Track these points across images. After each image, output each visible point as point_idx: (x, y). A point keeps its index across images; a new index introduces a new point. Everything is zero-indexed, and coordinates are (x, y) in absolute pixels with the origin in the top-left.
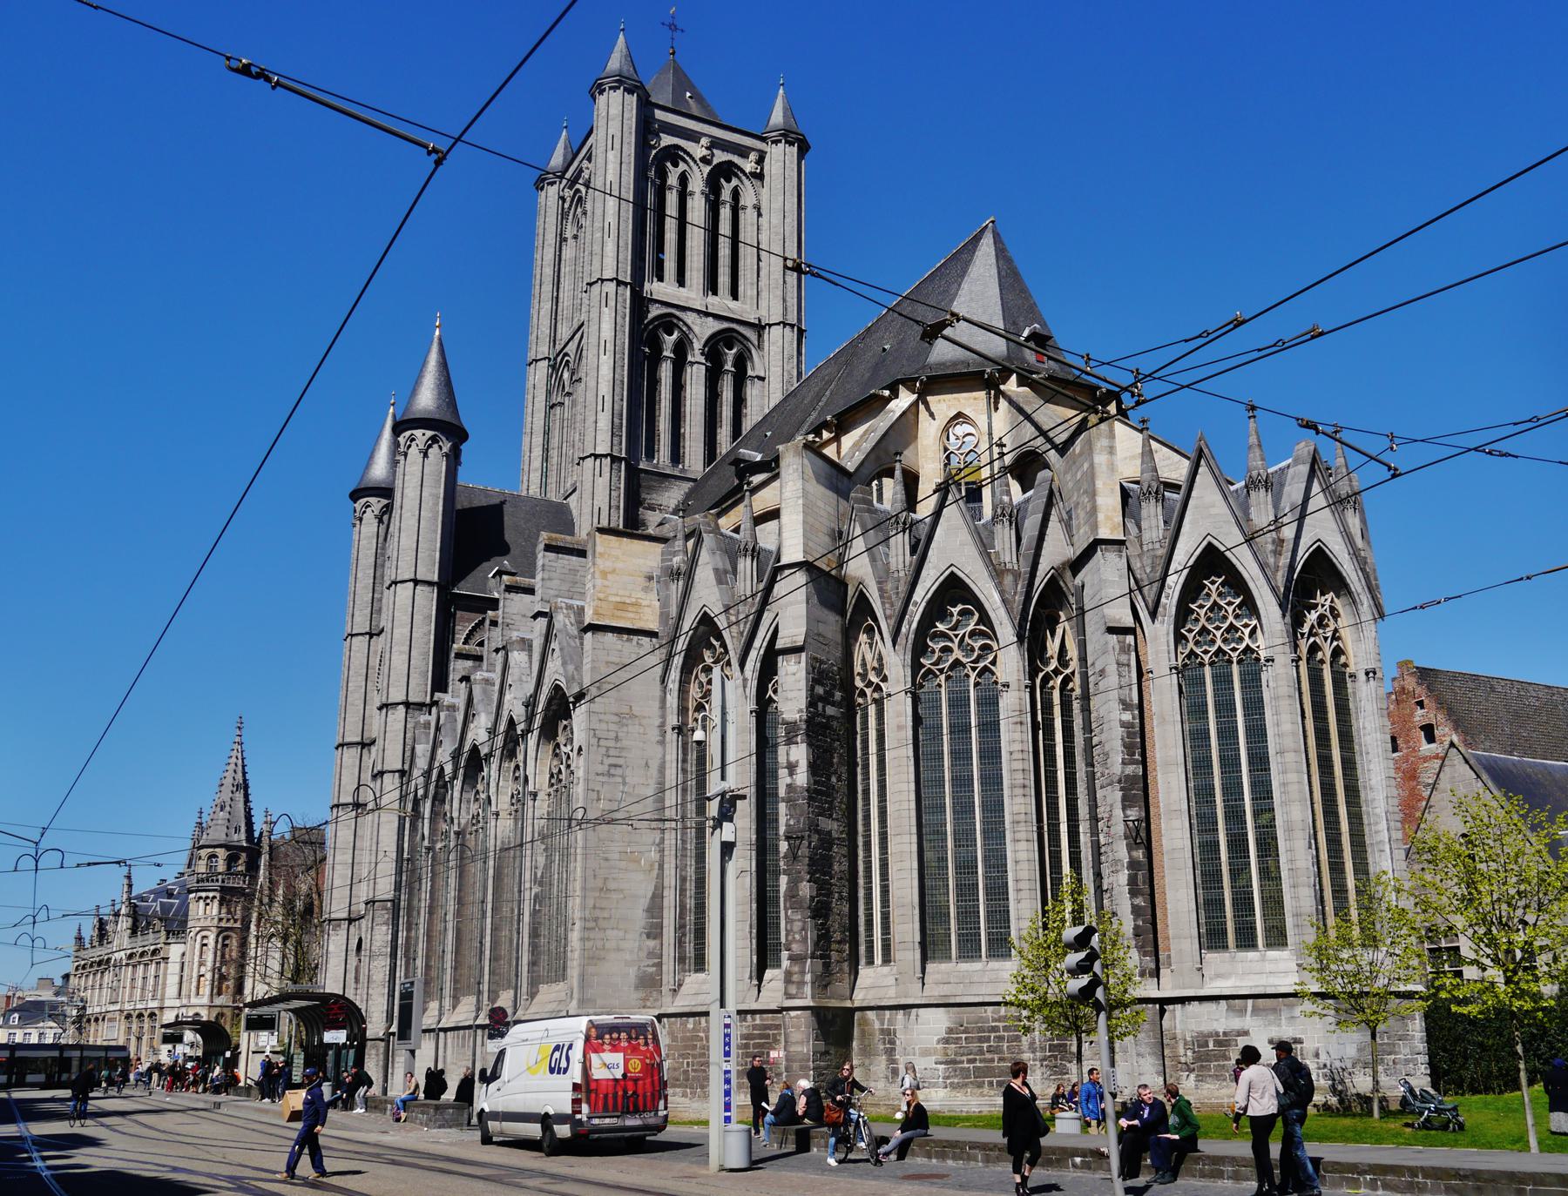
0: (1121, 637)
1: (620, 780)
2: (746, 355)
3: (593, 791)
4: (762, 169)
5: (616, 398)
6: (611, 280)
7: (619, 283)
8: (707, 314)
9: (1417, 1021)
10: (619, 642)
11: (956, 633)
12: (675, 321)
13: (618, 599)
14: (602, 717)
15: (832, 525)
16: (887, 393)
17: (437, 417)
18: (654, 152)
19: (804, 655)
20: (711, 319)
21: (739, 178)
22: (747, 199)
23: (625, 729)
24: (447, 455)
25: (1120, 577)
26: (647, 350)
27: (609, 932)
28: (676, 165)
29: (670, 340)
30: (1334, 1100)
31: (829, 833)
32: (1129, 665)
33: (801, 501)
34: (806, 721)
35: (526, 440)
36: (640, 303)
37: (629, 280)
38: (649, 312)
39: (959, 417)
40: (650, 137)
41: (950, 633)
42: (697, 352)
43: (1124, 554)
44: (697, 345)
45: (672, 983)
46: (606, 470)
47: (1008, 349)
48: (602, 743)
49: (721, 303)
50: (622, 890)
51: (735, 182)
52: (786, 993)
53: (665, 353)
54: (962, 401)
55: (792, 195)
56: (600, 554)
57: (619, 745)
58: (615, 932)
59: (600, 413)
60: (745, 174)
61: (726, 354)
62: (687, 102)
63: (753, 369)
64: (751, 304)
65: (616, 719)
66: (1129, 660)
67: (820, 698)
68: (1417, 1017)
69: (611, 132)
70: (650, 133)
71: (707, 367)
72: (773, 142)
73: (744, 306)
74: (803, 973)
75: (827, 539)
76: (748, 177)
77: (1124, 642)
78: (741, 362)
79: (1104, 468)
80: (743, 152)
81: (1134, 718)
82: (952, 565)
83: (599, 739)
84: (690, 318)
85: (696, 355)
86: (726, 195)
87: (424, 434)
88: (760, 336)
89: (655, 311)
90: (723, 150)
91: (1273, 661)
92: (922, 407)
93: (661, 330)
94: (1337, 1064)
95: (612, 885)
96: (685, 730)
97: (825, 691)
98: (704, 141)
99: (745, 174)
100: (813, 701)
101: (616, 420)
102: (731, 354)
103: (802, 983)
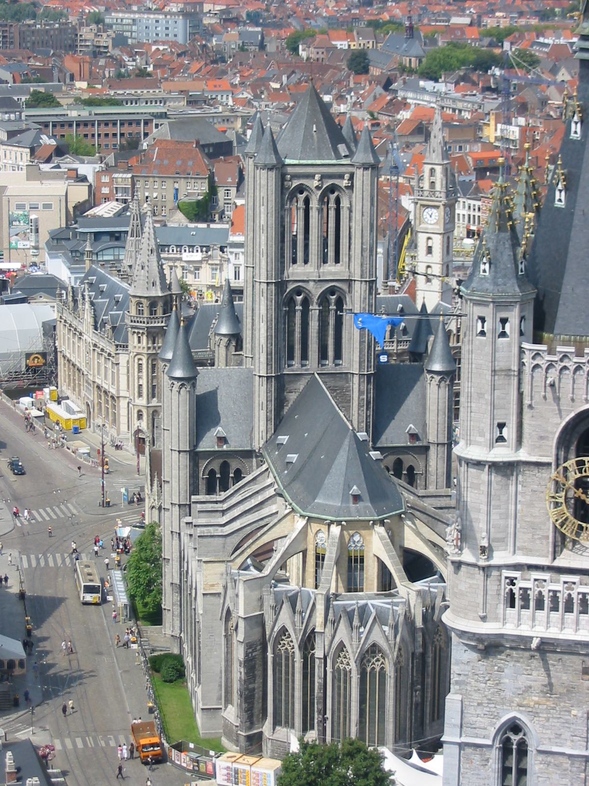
2: (342, 297)
4: (352, 183)
22: (344, 203)
36: (281, 285)
51: (336, 194)
53: (297, 308)
62: (312, 136)
63: (346, 304)
69: (262, 195)
70: (286, 181)
75: (255, 603)
78: (340, 303)
88: (350, 286)
89: (291, 287)
98: (317, 177)
100: (246, 654)
102: (333, 298)
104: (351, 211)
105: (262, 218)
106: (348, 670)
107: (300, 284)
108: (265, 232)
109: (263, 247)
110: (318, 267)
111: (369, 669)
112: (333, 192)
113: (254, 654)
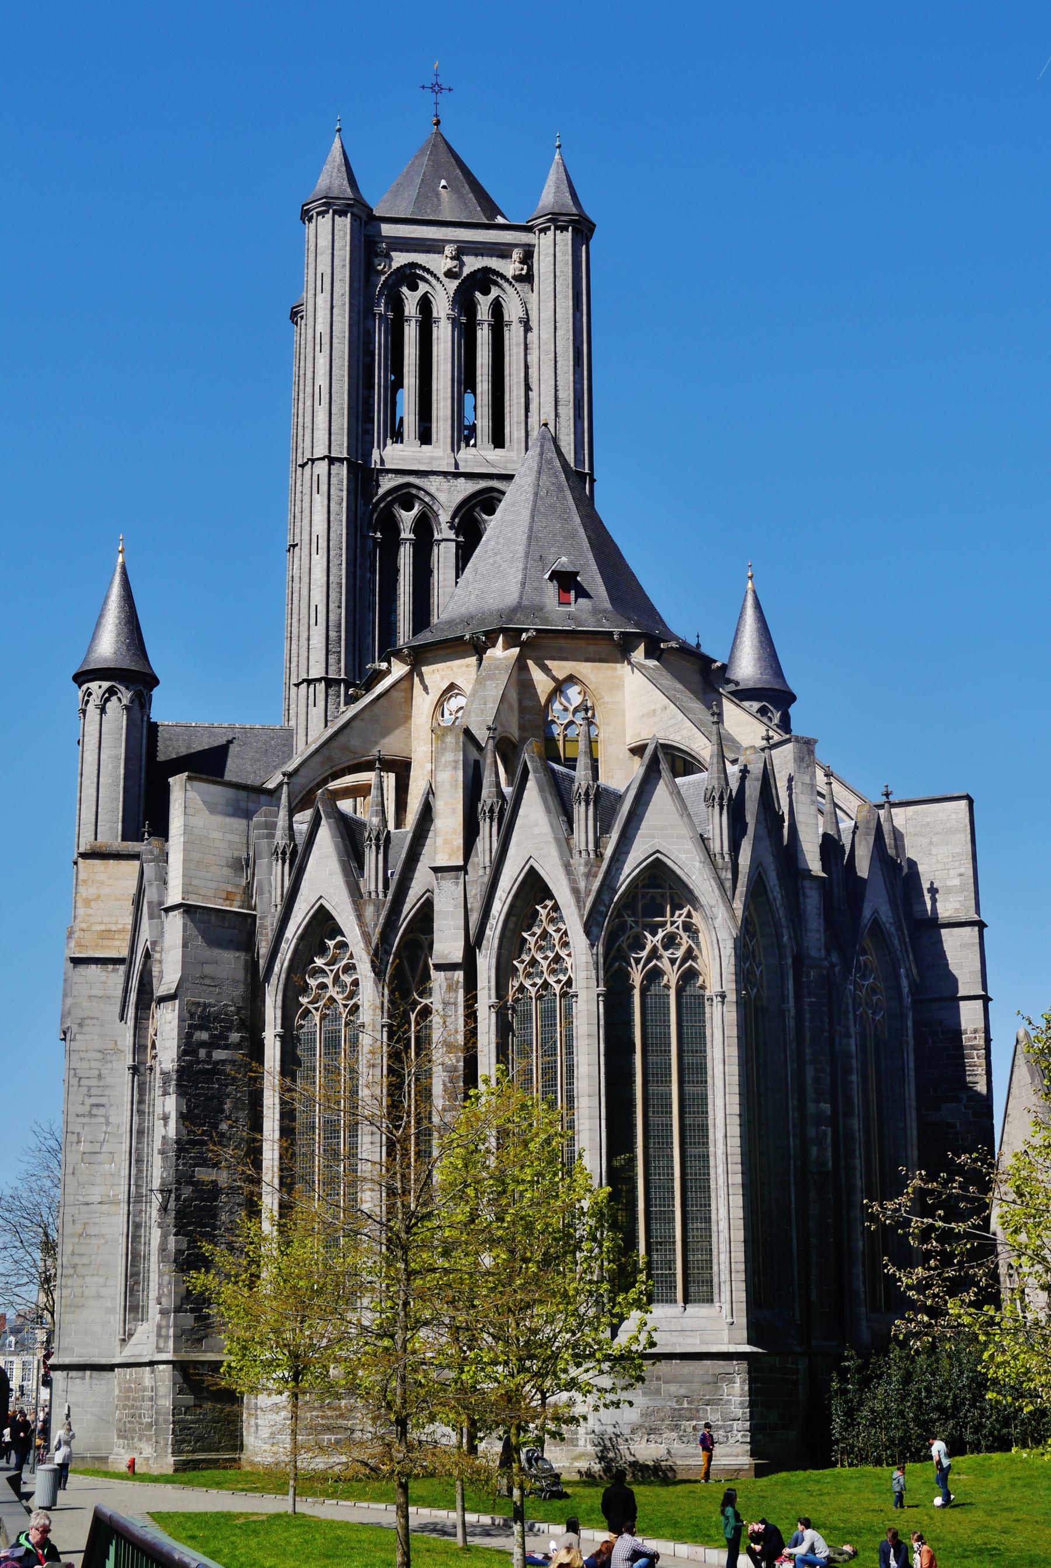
0: (449, 974)
1: (102, 1120)
3: (73, 1133)
4: (530, 268)
5: (332, 606)
6: (322, 459)
7: (332, 461)
8: (457, 475)
9: (737, 1385)
10: (104, 973)
11: (332, 968)
12: (414, 491)
13: (103, 927)
14: (82, 1055)
15: (236, 854)
16: (384, 665)
17: (112, 665)
18: (383, 278)
19: (177, 1001)
20: (462, 480)
21: (500, 286)
22: (512, 312)
23: (109, 1066)
24: (127, 708)
25: (456, 906)
26: (379, 535)
27: (89, 1279)
28: (414, 288)
29: (407, 518)
30: (597, 1467)
31: (214, 1183)
32: (455, 1004)
33: (182, 839)
34: (177, 1071)
35: (287, 643)
37: (345, 456)
38: (378, 486)
39: (451, 689)
40: (376, 261)
41: (326, 968)
42: (445, 526)
43: (462, 881)
44: (444, 517)
45: (122, 1331)
46: (321, 696)
47: (521, 597)
48: (83, 1082)
49: (471, 458)
50: (103, 1236)
52: (157, 1347)
53: (403, 535)
54: (456, 670)
55: (566, 297)
56: (84, 881)
57: (102, 1083)
58: (95, 1279)
59: (313, 627)
60: (507, 280)
61: (485, 521)
62: (438, 195)
64: (519, 450)
65: (99, 1056)
66: (456, 998)
67: (202, 1044)
68: (738, 1380)
70: (377, 255)
71: (457, 543)
72: (541, 231)
73: (510, 454)
74: (168, 1327)
75: (227, 871)
76: (511, 283)
77: (452, 979)
79: (447, 786)
80: (502, 251)
81: (458, 1061)
82: (321, 897)
83: (80, 1078)
84: (432, 484)
85: (444, 531)
86: (483, 312)
87: (100, 687)
89: (387, 483)
90: (476, 255)
91: (577, 996)
92: (416, 680)
93: (396, 506)
94: (610, 1430)
95: (92, 1230)
96: (142, 1069)
97: (212, 1036)
99: (507, 280)
100: (188, 1048)
101: (333, 634)
103: (168, 1337)
104: (527, 329)
105: (319, 320)
106: (557, 988)
107: (411, 479)
108: (326, 348)
109: (322, 380)
110: (455, 448)
111: (637, 977)
112: (486, 292)
113: (219, 1055)
